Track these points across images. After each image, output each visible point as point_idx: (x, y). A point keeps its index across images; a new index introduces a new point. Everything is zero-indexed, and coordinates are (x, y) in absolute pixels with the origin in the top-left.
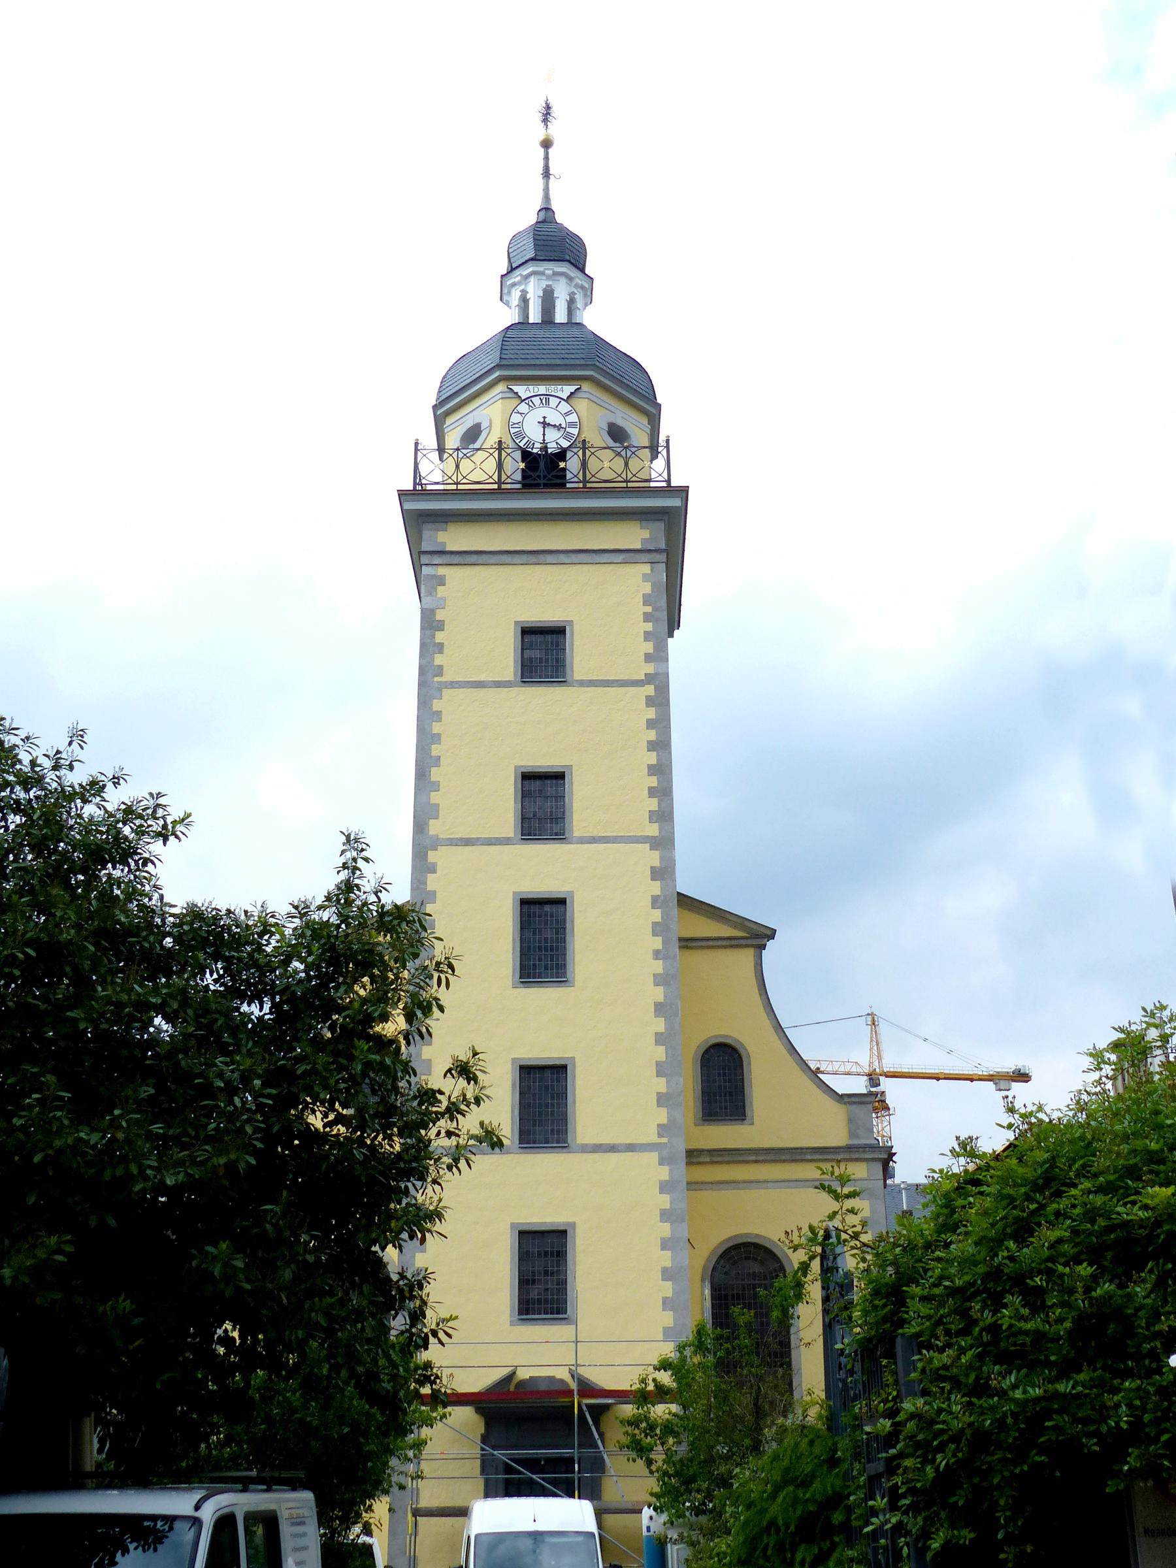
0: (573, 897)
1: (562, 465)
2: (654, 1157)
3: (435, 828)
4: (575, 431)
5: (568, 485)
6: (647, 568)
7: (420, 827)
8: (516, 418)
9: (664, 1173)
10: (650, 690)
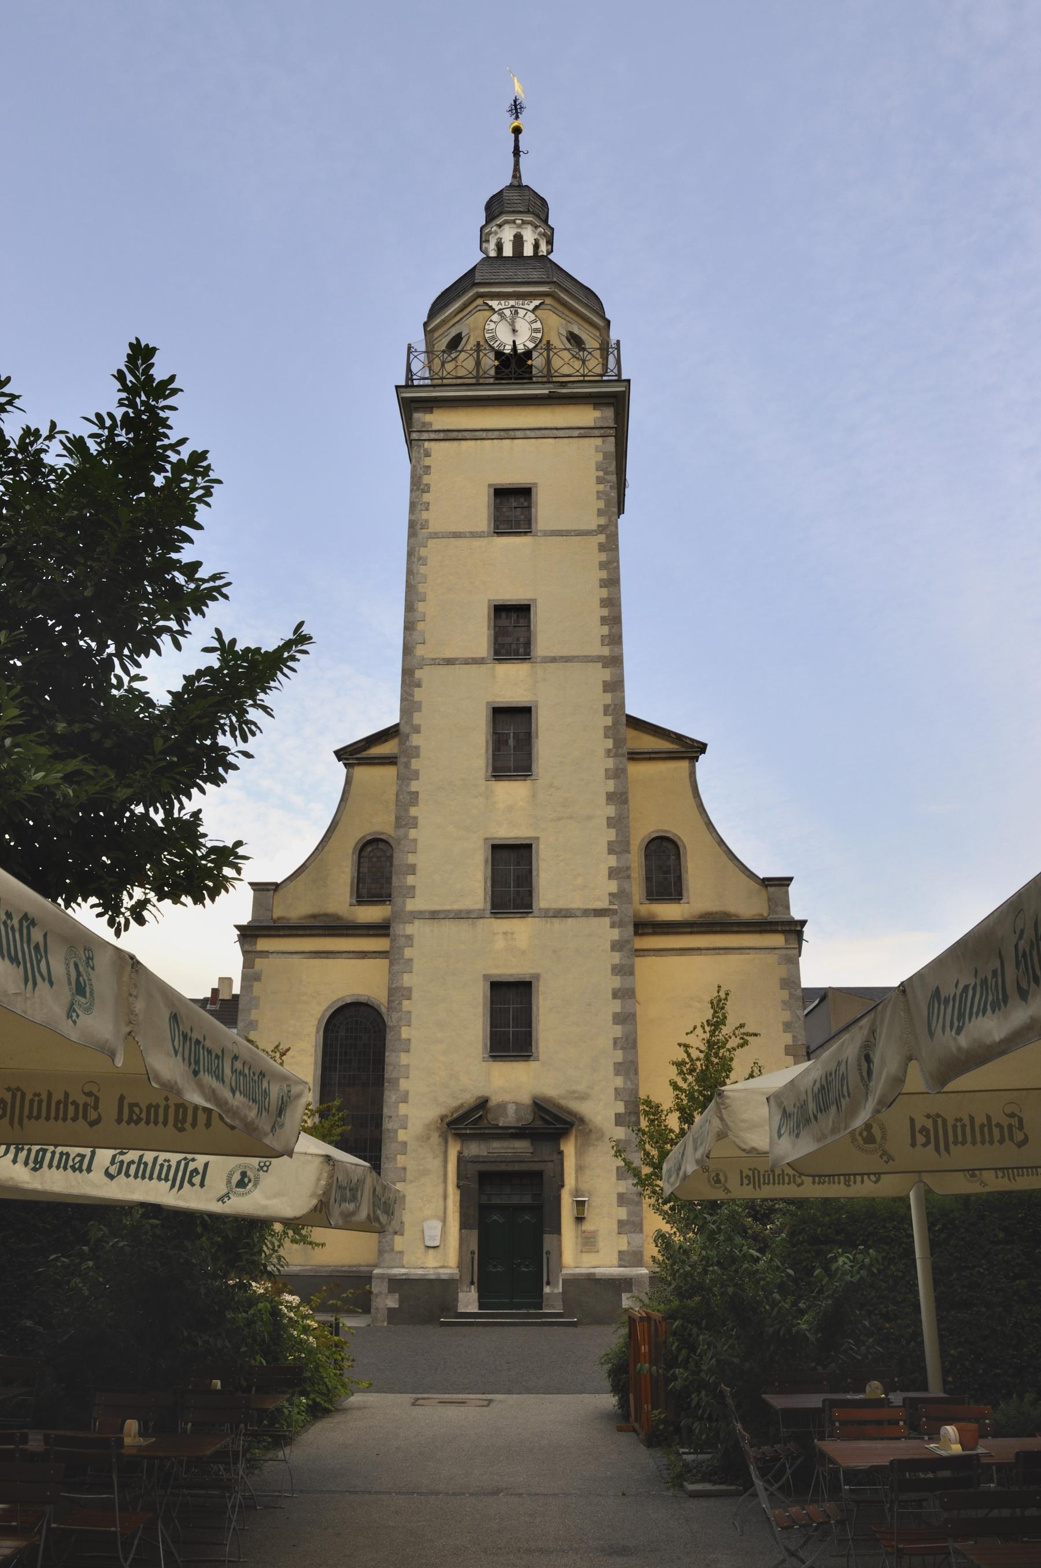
0: (537, 706)
1: (529, 362)
2: (607, 921)
3: (420, 651)
4: (539, 335)
5: (534, 379)
6: (599, 441)
7: (408, 650)
8: (492, 326)
9: (615, 934)
10: (602, 538)
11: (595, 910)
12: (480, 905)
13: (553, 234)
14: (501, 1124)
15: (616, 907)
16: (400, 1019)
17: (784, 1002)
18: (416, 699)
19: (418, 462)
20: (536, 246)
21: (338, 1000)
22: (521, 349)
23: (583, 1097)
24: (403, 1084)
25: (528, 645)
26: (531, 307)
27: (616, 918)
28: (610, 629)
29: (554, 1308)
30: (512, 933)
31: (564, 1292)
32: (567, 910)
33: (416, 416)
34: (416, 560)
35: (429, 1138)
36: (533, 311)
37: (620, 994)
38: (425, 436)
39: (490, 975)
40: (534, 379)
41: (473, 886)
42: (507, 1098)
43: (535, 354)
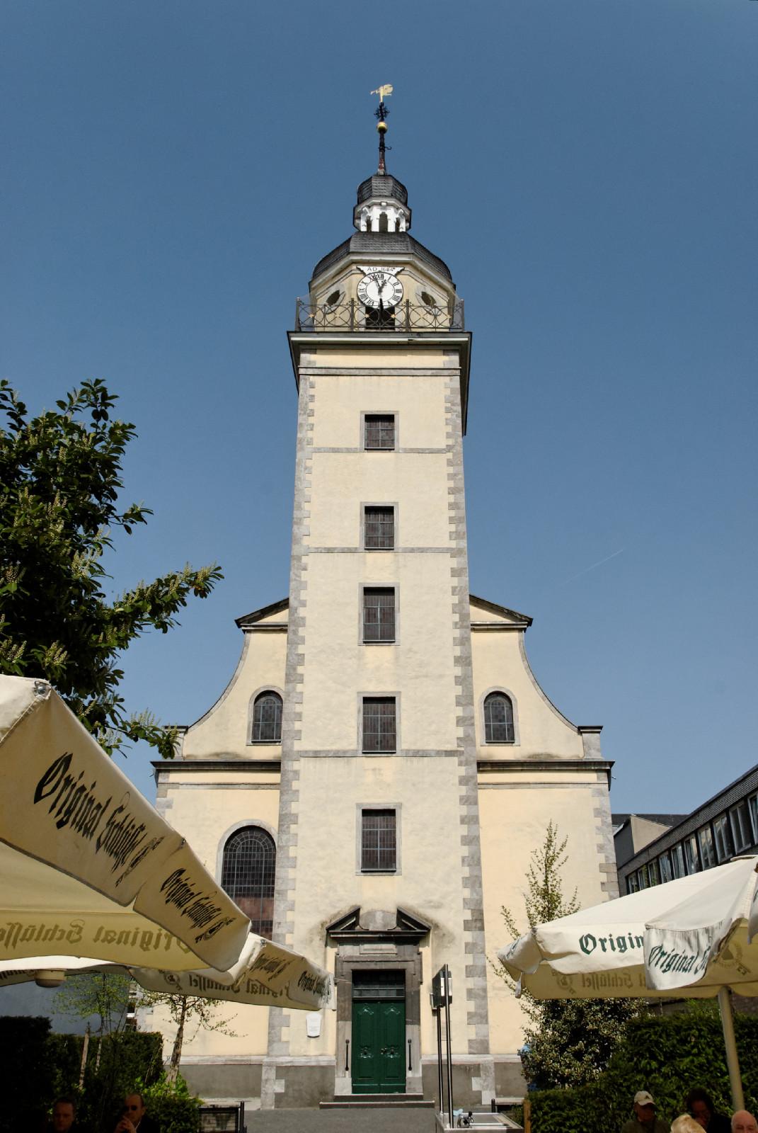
0: (399, 587)
2: (455, 760)
5: (397, 330)
6: (448, 379)
8: (363, 286)
9: (462, 771)
10: (450, 455)
11: (446, 751)
12: (354, 747)
13: (411, 214)
14: (371, 929)
15: (462, 749)
16: (288, 840)
17: (598, 828)
18: (303, 579)
19: (305, 392)
20: (398, 224)
21: (235, 824)
22: (386, 305)
23: (438, 906)
24: (291, 895)
25: (391, 538)
26: (394, 272)
27: (463, 758)
28: (456, 527)
29: (415, 1091)
30: (380, 770)
31: (424, 1077)
32: (423, 751)
33: (303, 356)
34: (303, 469)
35: (311, 941)
36: (396, 276)
37: (466, 820)
38: (310, 371)
39: (362, 804)
40: (397, 330)
41: (350, 732)
42: (376, 906)
43: (397, 310)
